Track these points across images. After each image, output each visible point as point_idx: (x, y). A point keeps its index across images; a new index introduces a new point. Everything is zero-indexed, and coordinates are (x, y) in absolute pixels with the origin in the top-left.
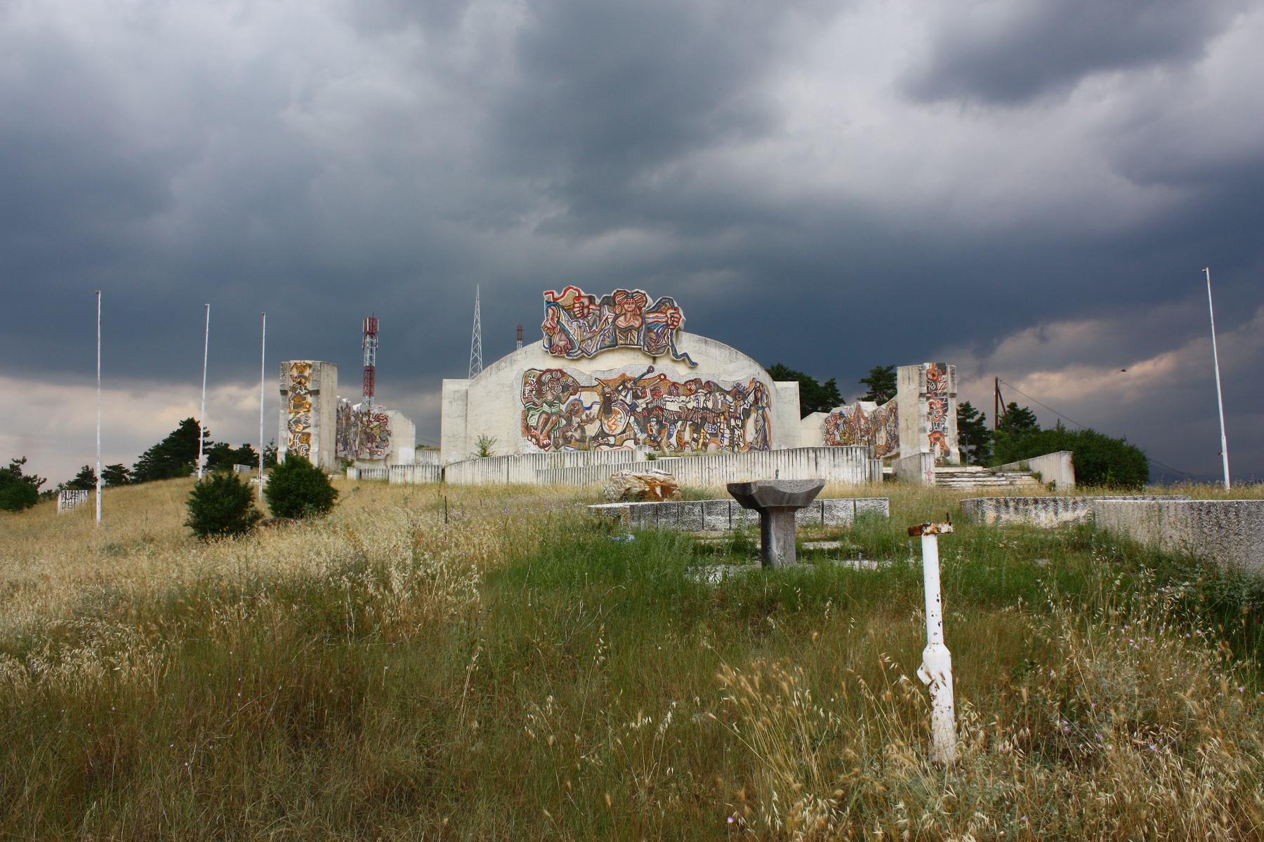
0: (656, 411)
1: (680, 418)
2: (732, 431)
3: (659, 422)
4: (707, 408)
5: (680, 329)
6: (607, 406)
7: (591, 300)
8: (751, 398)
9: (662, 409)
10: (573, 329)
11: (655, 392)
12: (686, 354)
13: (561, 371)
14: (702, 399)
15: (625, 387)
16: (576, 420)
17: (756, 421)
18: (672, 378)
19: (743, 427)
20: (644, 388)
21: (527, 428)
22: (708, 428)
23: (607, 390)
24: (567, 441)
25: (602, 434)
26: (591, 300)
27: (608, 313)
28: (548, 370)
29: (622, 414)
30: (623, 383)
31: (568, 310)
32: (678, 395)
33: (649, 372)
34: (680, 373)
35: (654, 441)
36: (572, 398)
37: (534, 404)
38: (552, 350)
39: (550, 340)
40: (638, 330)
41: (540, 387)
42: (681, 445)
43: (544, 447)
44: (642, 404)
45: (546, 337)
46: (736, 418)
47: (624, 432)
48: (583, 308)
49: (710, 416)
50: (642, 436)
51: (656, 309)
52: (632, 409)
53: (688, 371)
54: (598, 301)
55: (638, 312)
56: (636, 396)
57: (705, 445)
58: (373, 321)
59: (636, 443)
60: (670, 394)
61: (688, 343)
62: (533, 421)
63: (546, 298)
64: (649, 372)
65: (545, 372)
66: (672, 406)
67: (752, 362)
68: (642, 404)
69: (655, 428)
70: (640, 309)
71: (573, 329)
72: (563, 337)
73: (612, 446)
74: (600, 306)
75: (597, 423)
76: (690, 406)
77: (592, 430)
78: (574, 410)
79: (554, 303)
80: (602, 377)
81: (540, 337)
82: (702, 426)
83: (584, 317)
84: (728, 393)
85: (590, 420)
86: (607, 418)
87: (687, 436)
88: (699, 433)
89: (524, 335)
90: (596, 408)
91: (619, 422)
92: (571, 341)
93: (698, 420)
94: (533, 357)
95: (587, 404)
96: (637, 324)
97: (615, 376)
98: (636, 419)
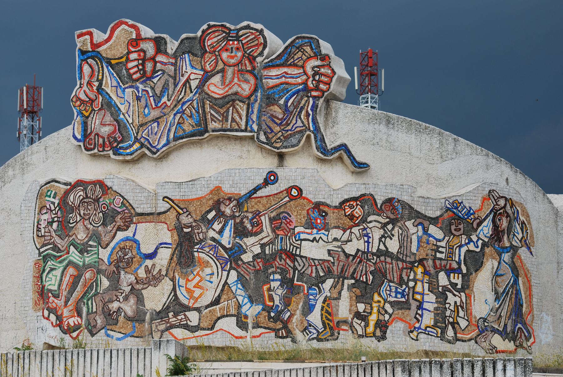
0: (281, 261)
1: (329, 273)
2: (442, 296)
3: (287, 283)
4: (387, 253)
5: (331, 99)
6: (185, 251)
7: (159, 44)
8: (486, 229)
9: (292, 257)
10: (125, 101)
11: (279, 222)
12: (344, 147)
13: (101, 183)
14: (377, 234)
15: (220, 214)
16: (126, 279)
17: (496, 275)
18: (312, 193)
19: (466, 287)
20: (257, 214)
21: (42, 294)
22: (388, 292)
23: (185, 220)
24: (111, 319)
25: (176, 306)
26: (159, 44)
27: (191, 71)
28: (80, 183)
29: (213, 267)
30: (217, 205)
31: (117, 65)
32: (326, 227)
33: (267, 182)
34: (333, 183)
35: (276, 319)
36: (120, 235)
37: (56, 248)
38: (88, 142)
39: (85, 125)
40: (248, 100)
41: (70, 211)
42: (332, 327)
43: (68, 331)
44: (252, 246)
45: (78, 120)
46: (449, 271)
47: (216, 302)
48: (144, 60)
49: (393, 268)
50: (252, 311)
51: (284, 60)
52: (234, 256)
53: (350, 179)
54: (172, 46)
55: (249, 66)
56: (241, 232)
57: (382, 326)
58: (33, 90)
59: (242, 325)
60: (310, 225)
61: (350, 124)
62: (51, 283)
63: (79, 43)
64: (267, 182)
65: (73, 186)
66: (314, 250)
67: (492, 160)
68: (252, 246)
69: (279, 293)
70: (252, 59)
71: (125, 101)
72: (108, 118)
73: (193, 329)
74: (175, 56)
75: (166, 285)
76: (350, 249)
77: (156, 298)
78: (123, 261)
79: (93, 54)
80: (176, 195)
81: (67, 121)
82: (376, 287)
83: (146, 78)
84: (434, 221)
85: (154, 279)
86: (185, 275)
87: (344, 309)
88: (369, 302)
89: (44, 115)
90: (165, 255)
91: (207, 281)
92: (120, 126)
93: (368, 277)
94: (57, 159)
95: (147, 249)
96: (246, 89)
97: (200, 191)
98: (240, 277)
